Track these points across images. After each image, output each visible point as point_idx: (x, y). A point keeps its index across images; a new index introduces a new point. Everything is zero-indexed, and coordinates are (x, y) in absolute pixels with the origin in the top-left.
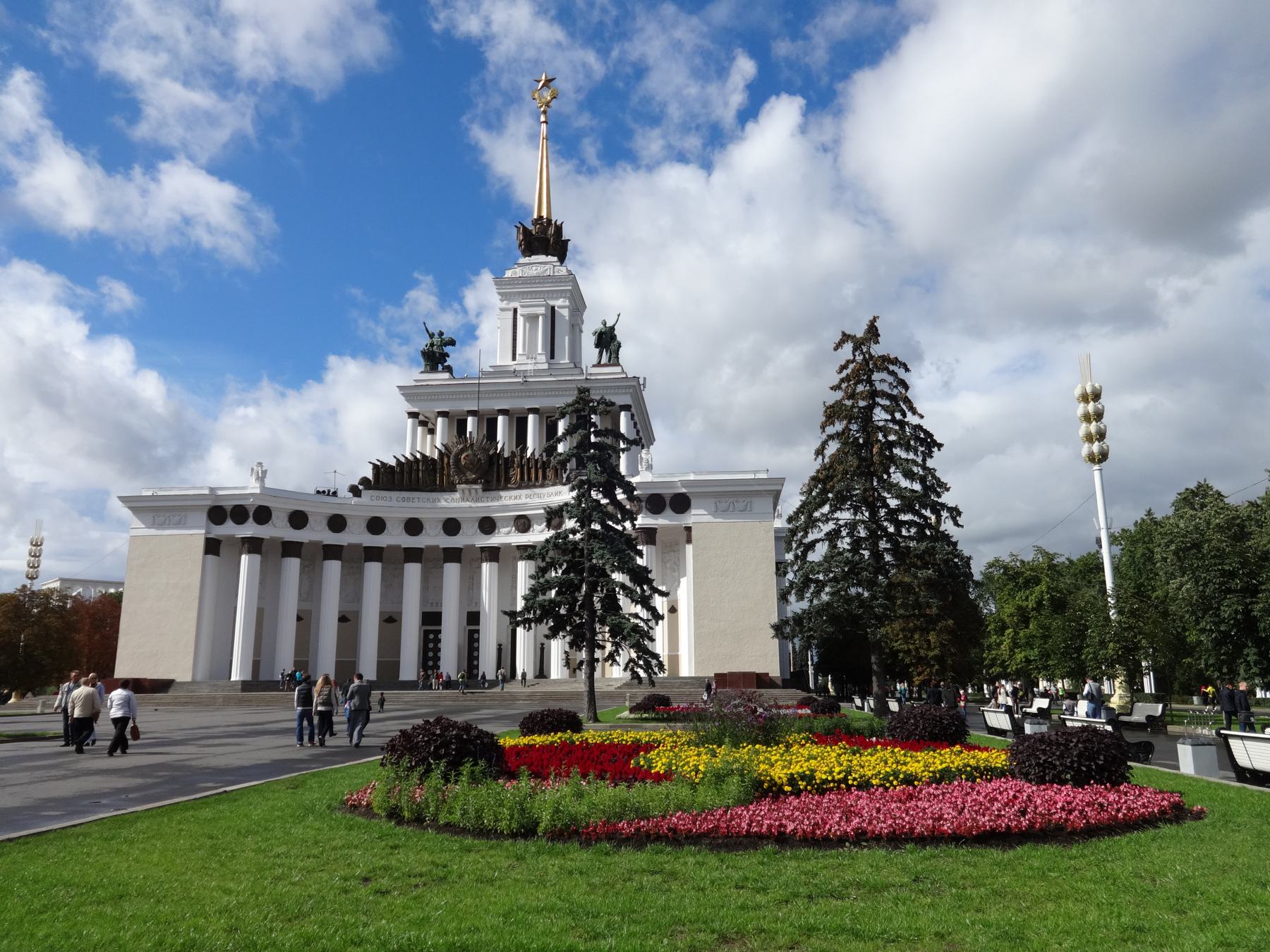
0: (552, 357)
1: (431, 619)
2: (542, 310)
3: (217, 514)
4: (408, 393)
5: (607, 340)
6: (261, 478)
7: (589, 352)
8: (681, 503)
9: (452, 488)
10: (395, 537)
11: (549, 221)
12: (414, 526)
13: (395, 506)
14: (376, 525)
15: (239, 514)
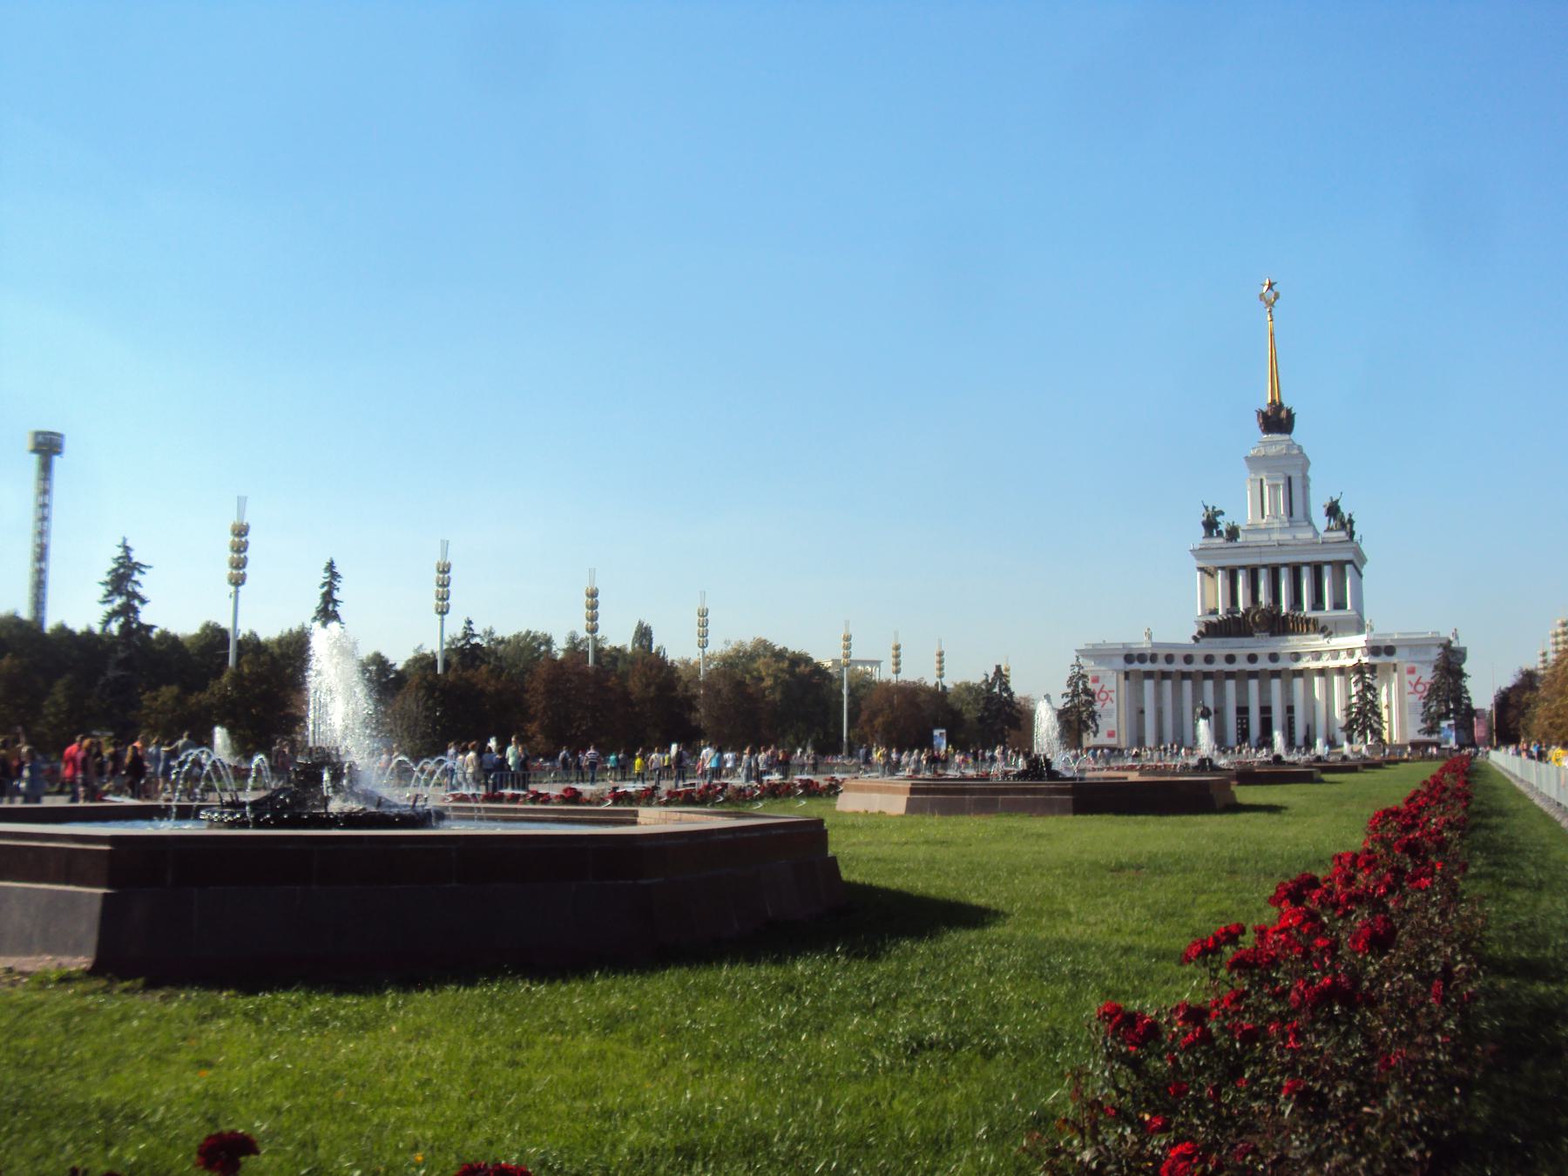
0: (1291, 514)
1: (1243, 711)
2: (1281, 482)
3: (1129, 658)
4: (1198, 553)
5: (1333, 510)
6: (1150, 637)
7: (1321, 520)
8: (1390, 651)
9: (1251, 635)
10: (1220, 665)
11: (1281, 405)
12: (1230, 659)
13: (1220, 647)
14: (1209, 659)
15: (1142, 658)
